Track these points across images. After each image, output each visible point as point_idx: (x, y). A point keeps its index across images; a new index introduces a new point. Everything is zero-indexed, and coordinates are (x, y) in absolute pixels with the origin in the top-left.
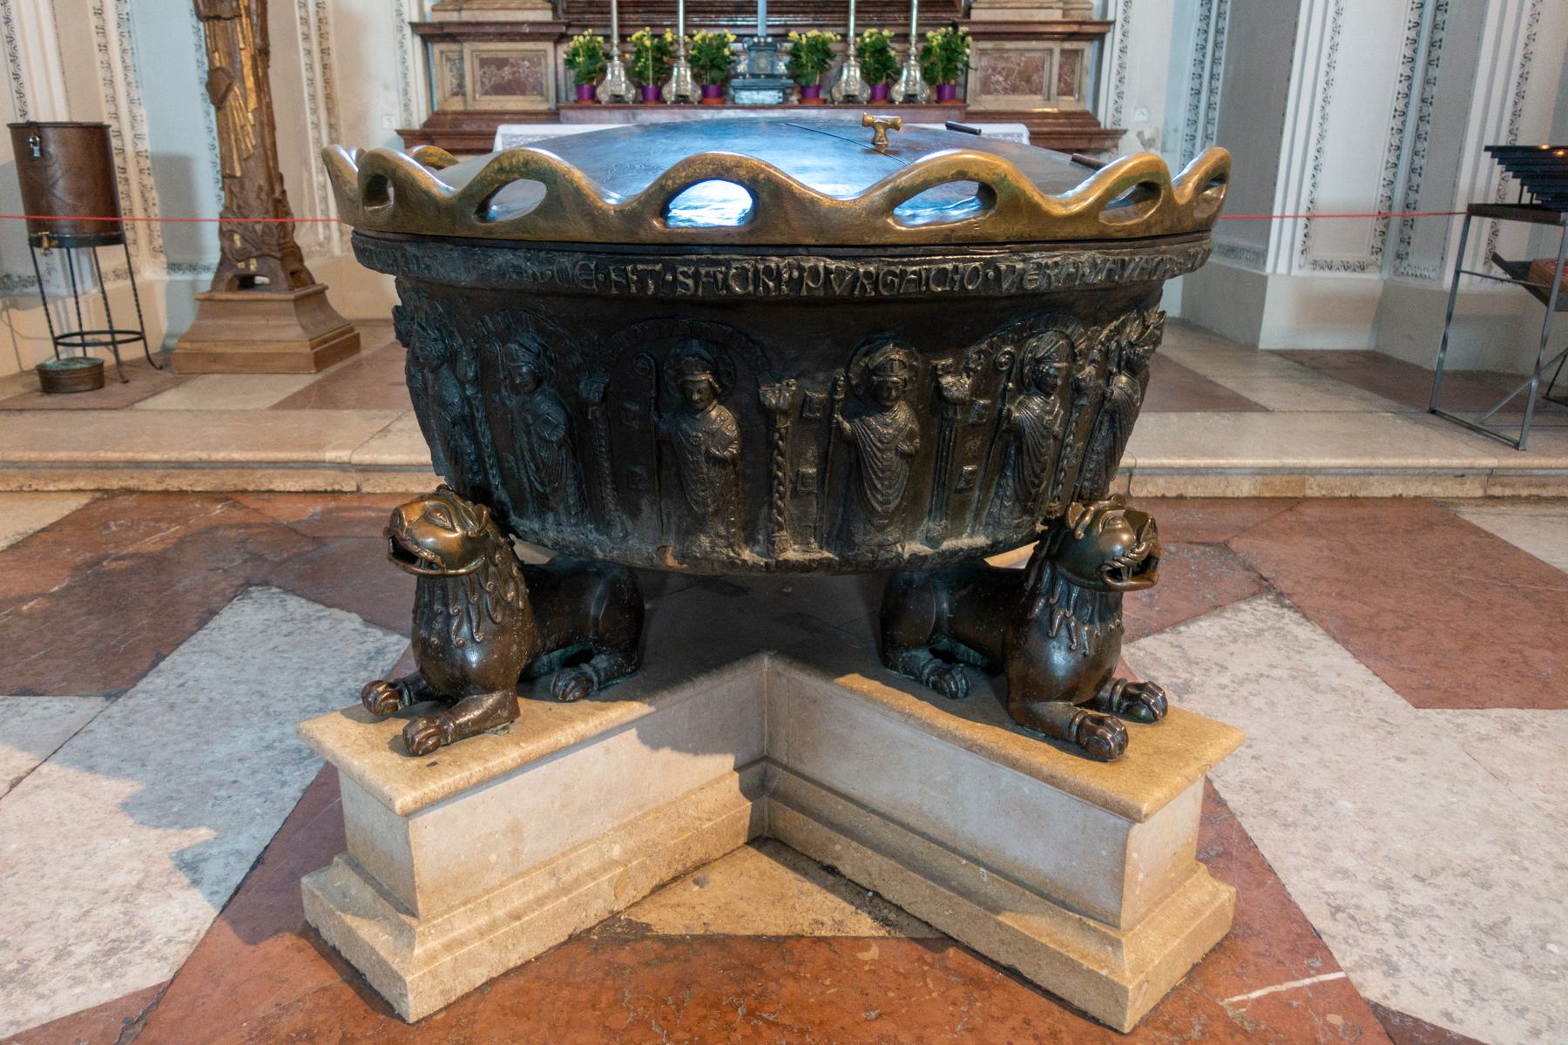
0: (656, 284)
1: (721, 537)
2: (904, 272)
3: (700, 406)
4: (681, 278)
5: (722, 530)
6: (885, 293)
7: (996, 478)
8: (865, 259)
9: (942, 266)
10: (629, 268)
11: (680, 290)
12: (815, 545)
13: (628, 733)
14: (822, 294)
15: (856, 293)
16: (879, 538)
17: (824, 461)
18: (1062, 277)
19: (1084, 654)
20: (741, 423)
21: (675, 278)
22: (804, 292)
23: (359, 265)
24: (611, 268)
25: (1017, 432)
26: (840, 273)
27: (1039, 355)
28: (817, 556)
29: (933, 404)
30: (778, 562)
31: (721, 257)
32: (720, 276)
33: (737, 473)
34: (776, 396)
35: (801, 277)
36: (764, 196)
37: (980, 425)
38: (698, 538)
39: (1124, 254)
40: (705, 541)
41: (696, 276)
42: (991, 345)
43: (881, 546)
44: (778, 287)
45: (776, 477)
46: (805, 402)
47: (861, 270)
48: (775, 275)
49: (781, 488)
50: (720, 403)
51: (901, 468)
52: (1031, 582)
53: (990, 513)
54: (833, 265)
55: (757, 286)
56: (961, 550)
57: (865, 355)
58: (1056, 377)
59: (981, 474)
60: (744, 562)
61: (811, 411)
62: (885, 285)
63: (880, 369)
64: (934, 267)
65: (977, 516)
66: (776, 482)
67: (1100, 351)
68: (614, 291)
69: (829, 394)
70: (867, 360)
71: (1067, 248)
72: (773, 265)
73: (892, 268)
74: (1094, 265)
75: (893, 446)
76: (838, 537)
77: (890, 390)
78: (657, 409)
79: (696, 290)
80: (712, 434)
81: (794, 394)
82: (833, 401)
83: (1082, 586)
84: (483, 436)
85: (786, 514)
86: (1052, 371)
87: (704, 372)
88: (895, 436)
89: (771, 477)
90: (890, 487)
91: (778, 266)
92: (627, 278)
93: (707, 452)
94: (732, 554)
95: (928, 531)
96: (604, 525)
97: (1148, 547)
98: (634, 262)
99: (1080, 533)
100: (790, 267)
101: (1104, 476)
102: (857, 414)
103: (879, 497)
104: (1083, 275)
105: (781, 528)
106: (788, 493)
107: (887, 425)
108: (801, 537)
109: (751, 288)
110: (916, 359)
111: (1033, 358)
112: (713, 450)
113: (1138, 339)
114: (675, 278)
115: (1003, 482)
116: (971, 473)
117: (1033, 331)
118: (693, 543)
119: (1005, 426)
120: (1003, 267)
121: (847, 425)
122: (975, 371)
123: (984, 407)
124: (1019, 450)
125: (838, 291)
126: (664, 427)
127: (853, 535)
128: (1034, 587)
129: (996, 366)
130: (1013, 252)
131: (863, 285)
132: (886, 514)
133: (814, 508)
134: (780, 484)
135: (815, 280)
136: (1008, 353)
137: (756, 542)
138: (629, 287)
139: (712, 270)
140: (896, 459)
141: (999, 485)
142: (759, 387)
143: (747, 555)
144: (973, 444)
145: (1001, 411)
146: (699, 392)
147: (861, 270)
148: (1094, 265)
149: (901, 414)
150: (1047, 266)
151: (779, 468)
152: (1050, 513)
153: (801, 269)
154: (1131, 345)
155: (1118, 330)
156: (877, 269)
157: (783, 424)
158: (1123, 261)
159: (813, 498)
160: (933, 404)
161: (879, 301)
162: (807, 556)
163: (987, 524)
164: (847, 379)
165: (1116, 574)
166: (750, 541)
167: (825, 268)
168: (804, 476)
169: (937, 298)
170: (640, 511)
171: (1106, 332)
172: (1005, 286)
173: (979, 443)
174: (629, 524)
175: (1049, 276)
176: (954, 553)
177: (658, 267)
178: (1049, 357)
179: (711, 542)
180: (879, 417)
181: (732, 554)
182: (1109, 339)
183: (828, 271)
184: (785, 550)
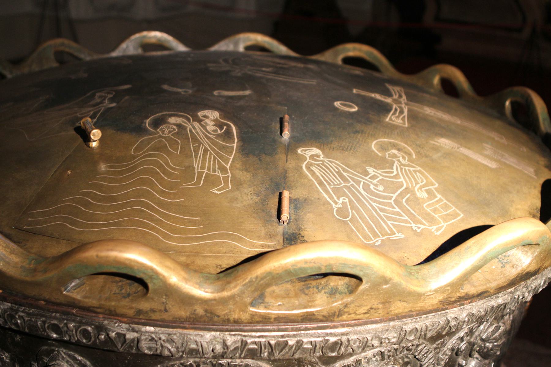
73: (13, 313)
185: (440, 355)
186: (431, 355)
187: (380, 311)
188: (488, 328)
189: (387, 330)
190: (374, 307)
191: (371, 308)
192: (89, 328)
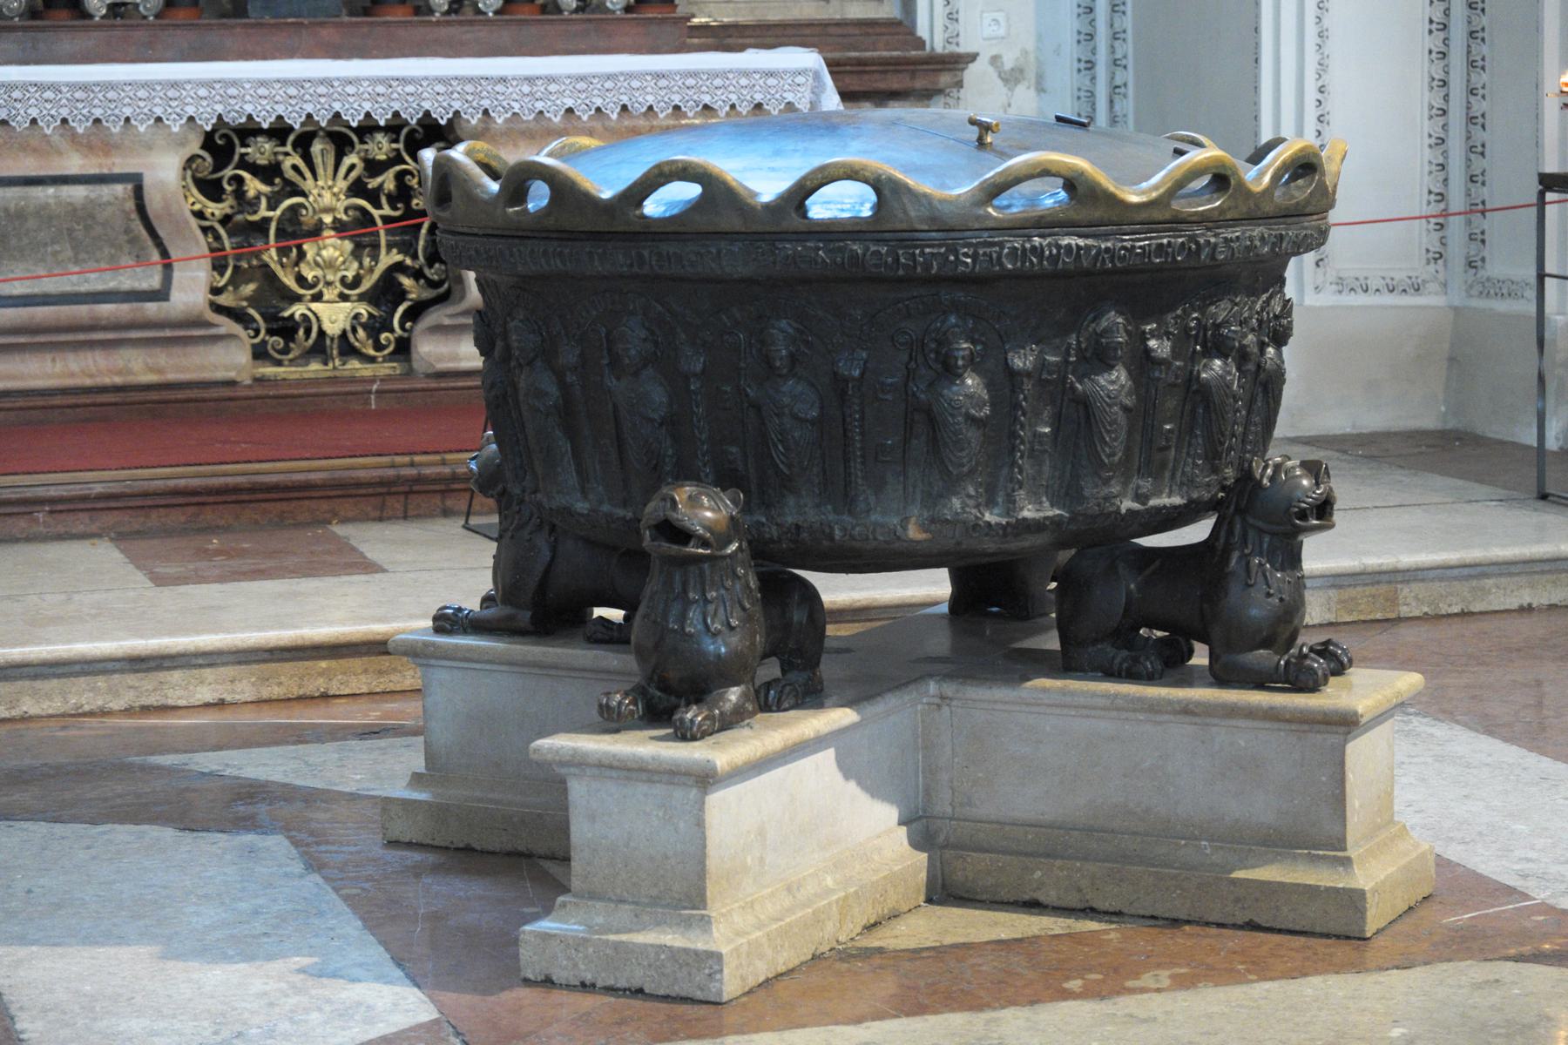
1: (969, 496)
2: (1133, 247)
3: (960, 371)
6: (1119, 265)
7: (1187, 438)
8: (1105, 236)
9: (1159, 241)
10: (917, 251)
11: (961, 268)
12: (1047, 504)
13: (820, 756)
14: (1073, 268)
15: (1098, 265)
16: (1105, 491)
17: (1057, 422)
18: (1242, 249)
19: (1281, 600)
20: (990, 385)
21: (957, 258)
22: (1060, 265)
24: (901, 252)
26: (1088, 248)
27: (1219, 321)
28: (1050, 514)
29: (1143, 363)
30: (1017, 520)
31: (996, 239)
32: (994, 255)
34: (1022, 361)
35: (1059, 252)
36: (886, 192)
38: (950, 500)
39: (1280, 229)
40: (956, 503)
41: (975, 257)
42: (1184, 311)
43: (1106, 499)
44: (1040, 262)
45: (1020, 436)
47: (1103, 246)
49: (1022, 447)
51: (1121, 418)
52: (1222, 541)
53: (1183, 473)
54: (1081, 242)
55: (1023, 263)
56: (1165, 507)
57: (1093, 322)
58: (1234, 339)
59: (1176, 432)
60: (989, 524)
61: (1050, 373)
63: (1106, 331)
64: (1154, 241)
65: (1173, 476)
67: (1257, 319)
68: (901, 272)
70: (1094, 325)
71: (1243, 225)
72: (1037, 244)
73: (1125, 244)
76: (1067, 494)
77: (1116, 349)
79: (974, 267)
80: (970, 396)
82: (1066, 362)
83: (1273, 534)
88: (1120, 391)
89: (1013, 435)
90: (1115, 440)
92: (915, 260)
94: (978, 514)
95: (1138, 487)
96: (847, 501)
97: (1325, 489)
99: (1265, 481)
100: (1049, 245)
101: (1262, 448)
102: (1084, 376)
103: (1107, 449)
107: (1113, 382)
109: (1019, 264)
111: (1213, 323)
112: (973, 411)
113: (1282, 310)
115: (1193, 441)
117: (1214, 299)
118: (944, 506)
119: (1195, 387)
120: (1202, 241)
122: (1174, 335)
123: (1179, 368)
124: (1207, 408)
125: (1085, 265)
127: (1082, 489)
128: (1227, 543)
129: (1187, 330)
130: (1209, 229)
133: (1046, 468)
134: (1022, 442)
136: (1196, 319)
137: (997, 504)
138: (915, 268)
139: (988, 250)
140: (1121, 413)
141: (1190, 444)
142: (1006, 353)
143: (988, 517)
144: (1171, 403)
145: (1191, 372)
147: (1103, 246)
148: (1262, 239)
150: (1231, 240)
151: (1022, 427)
152: (1225, 479)
153: (1059, 247)
154: (1276, 317)
155: (1268, 302)
156: (1114, 245)
157: (1028, 385)
158: (1281, 234)
159: (1046, 456)
160: (1143, 363)
161: (1114, 271)
162: (1041, 514)
163: (1182, 484)
164: (1079, 342)
165: (1303, 515)
166: (990, 503)
167: (1077, 245)
169: (1159, 269)
171: (1260, 302)
174: (872, 499)
175: (1233, 249)
176: (1158, 509)
177: (943, 250)
178: (1227, 322)
180: (1106, 376)
181: (978, 514)
182: (1263, 309)
184: (1022, 509)
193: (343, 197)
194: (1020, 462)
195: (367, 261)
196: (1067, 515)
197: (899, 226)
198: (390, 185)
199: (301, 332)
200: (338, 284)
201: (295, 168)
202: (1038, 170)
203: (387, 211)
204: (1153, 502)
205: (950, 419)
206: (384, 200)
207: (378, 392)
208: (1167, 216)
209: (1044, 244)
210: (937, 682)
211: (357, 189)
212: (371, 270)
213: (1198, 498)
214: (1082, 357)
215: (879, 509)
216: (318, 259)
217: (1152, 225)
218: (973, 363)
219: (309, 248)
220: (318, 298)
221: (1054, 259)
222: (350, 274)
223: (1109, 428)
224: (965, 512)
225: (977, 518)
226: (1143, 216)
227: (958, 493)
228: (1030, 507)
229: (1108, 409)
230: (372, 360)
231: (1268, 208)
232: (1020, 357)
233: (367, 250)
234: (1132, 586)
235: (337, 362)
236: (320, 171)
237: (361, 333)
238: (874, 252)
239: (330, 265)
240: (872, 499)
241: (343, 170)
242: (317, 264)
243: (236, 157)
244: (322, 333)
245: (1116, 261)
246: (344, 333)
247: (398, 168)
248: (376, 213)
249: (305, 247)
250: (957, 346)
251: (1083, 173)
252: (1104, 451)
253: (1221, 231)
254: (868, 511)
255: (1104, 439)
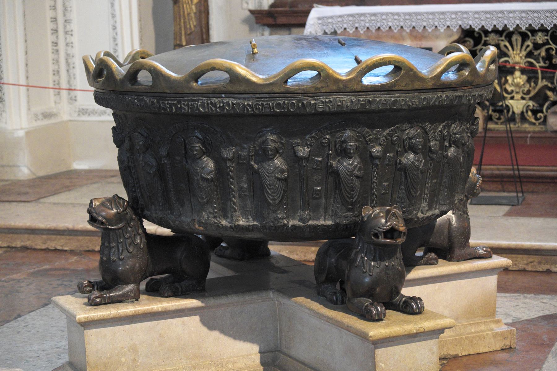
0: (176, 108)
1: (210, 213)
4: (183, 106)
5: (211, 211)
7: (333, 194)
12: (251, 219)
21: (181, 106)
23: (96, 104)
24: (161, 102)
25: (336, 173)
26: (238, 104)
30: (235, 226)
31: (195, 98)
32: (196, 106)
33: (216, 186)
34: (228, 153)
35: (223, 105)
37: (318, 169)
38: (202, 213)
40: (205, 215)
41: (188, 105)
44: (216, 109)
45: (231, 187)
46: (239, 156)
48: (214, 105)
50: (208, 156)
56: (318, 226)
58: (350, 149)
60: (222, 225)
62: (256, 109)
65: (325, 211)
66: (231, 190)
68: (162, 111)
69: (248, 153)
71: (336, 95)
72: (213, 101)
73: (258, 103)
74: (352, 102)
75: (273, 175)
78: (186, 158)
81: (234, 153)
84: (134, 174)
85: (238, 204)
86: (349, 147)
87: (198, 143)
91: (215, 102)
92: (166, 106)
93: (201, 175)
98: (168, 100)
100: (220, 102)
103: (270, 197)
104: (347, 106)
105: (235, 210)
106: (237, 196)
108: (245, 215)
109: (207, 110)
110: (282, 139)
114: (181, 106)
116: (320, 190)
120: (305, 102)
121: (256, 166)
126: (187, 166)
130: (310, 97)
131: (247, 108)
132: (275, 205)
133: (249, 202)
135: (229, 107)
139: (193, 103)
141: (335, 198)
143: (224, 223)
144: (317, 177)
146: (196, 151)
149: (278, 162)
150: (326, 102)
151: (232, 184)
162: (247, 224)
163: (332, 215)
164: (254, 147)
166: (225, 217)
167: (232, 103)
168: (242, 187)
170: (184, 203)
172: (308, 110)
173: (320, 177)
174: (181, 209)
175: (328, 106)
177: (175, 102)
179: (208, 215)
183: (233, 104)
185: (436, 134)
186: (432, 132)
187: (410, 85)
188: (456, 127)
189: (414, 97)
190: (408, 83)
191: (407, 84)
192: (294, 101)
193: (523, 58)
194: (233, 199)
195: (533, 84)
196: (259, 225)
197: (159, 91)
198: (543, 54)
199: (505, 111)
200: (521, 93)
201: (505, 46)
202: (210, 67)
203: (542, 64)
204: (310, 223)
205: (195, 178)
206: (541, 60)
207: (531, 137)
208: (282, 90)
209: (216, 101)
210: (273, 293)
211: (530, 55)
212: (534, 88)
213: (339, 222)
214: (257, 154)
215: (184, 214)
216: (513, 83)
217: (272, 95)
218: (208, 153)
219: (509, 78)
220: (512, 98)
221: (222, 108)
222: (526, 89)
223: (269, 187)
224: (208, 219)
225: (215, 223)
226: (267, 90)
227: (206, 211)
228: (244, 220)
229: (267, 178)
230: (534, 124)
231: (355, 87)
232: (226, 152)
233: (533, 80)
234: (333, 260)
235: (520, 124)
236: (515, 47)
237: (530, 113)
238: (152, 101)
239: (517, 85)
240: (181, 209)
241: (524, 47)
242: (512, 84)
243: (483, 42)
244: (513, 112)
245: (254, 110)
246: (522, 112)
247: (547, 47)
248: (537, 65)
249: (508, 78)
250: (192, 145)
251: (231, 69)
252: (269, 198)
253: (318, 98)
254: (180, 215)
255: (268, 192)
